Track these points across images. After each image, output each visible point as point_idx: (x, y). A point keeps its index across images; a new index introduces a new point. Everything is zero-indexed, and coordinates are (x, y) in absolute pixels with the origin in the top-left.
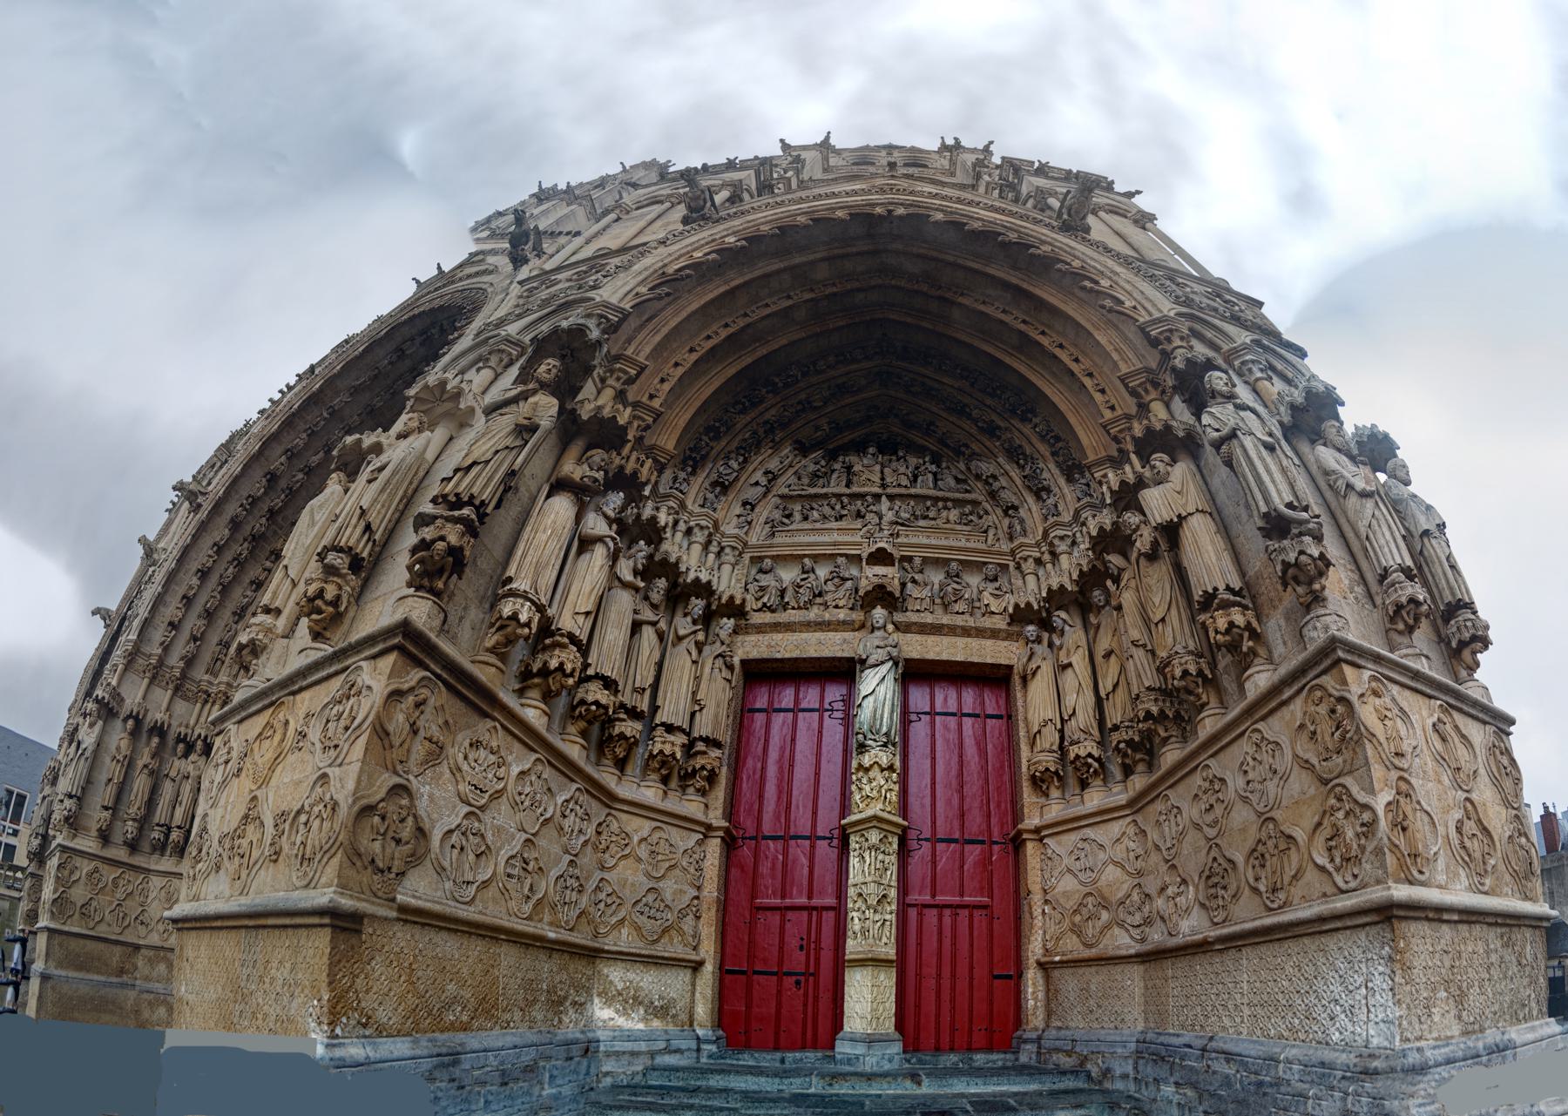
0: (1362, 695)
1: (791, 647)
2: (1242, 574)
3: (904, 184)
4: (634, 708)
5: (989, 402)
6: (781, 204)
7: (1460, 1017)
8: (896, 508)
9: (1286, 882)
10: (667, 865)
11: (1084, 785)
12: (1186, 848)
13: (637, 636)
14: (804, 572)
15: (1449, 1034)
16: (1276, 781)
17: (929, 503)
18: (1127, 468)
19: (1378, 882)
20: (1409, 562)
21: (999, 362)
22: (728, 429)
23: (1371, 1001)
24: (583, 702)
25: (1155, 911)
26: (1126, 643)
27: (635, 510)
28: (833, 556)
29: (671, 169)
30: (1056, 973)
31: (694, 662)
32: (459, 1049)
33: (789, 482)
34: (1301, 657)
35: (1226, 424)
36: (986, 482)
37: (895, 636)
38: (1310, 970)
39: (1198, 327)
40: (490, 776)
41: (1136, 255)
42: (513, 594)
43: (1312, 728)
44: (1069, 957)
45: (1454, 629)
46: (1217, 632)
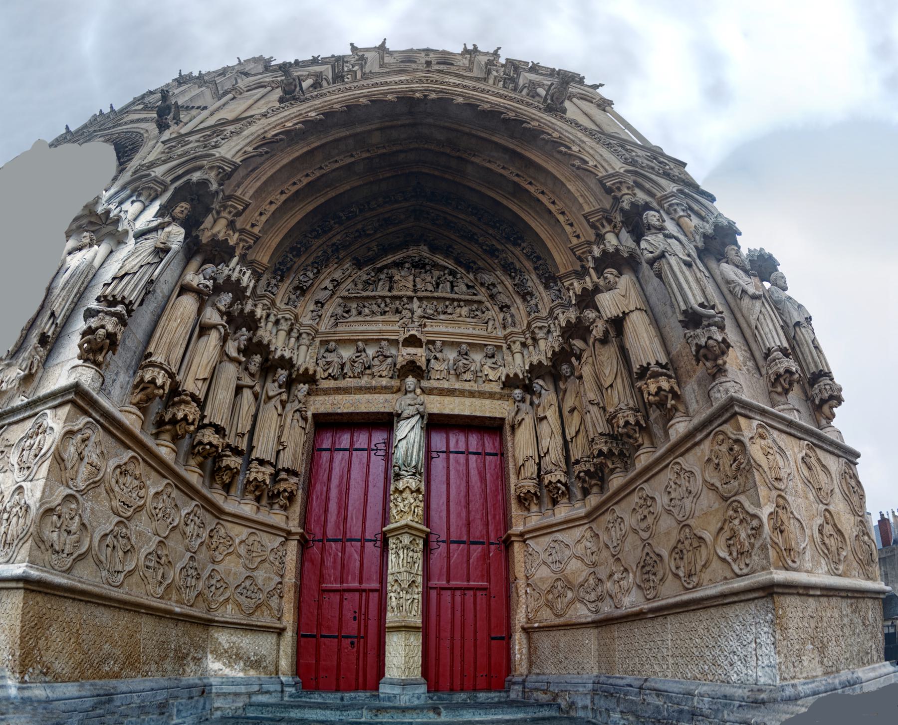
0: (752, 438)
2: (668, 353)
3: (436, 76)
4: (237, 447)
5: (491, 232)
6: (349, 89)
7: (822, 663)
8: (424, 306)
9: (698, 567)
10: (259, 559)
11: (555, 502)
12: (627, 546)
15: (814, 674)
16: (691, 498)
17: (447, 303)
18: (588, 279)
19: (764, 569)
20: (785, 344)
21: (499, 204)
22: (306, 249)
23: (759, 652)
24: (200, 443)
25: (605, 591)
26: (585, 402)
27: (240, 306)
29: (273, 63)
30: (535, 636)
31: (279, 415)
32: (112, 691)
34: (709, 411)
35: (657, 248)
36: (488, 288)
37: (422, 397)
38: (716, 631)
39: (640, 180)
40: (134, 495)
41: (597, 129)
42: (152, 365)
43: (716, 461)
44: (545, 624)
45: (817, 391)
46: (649, 394)
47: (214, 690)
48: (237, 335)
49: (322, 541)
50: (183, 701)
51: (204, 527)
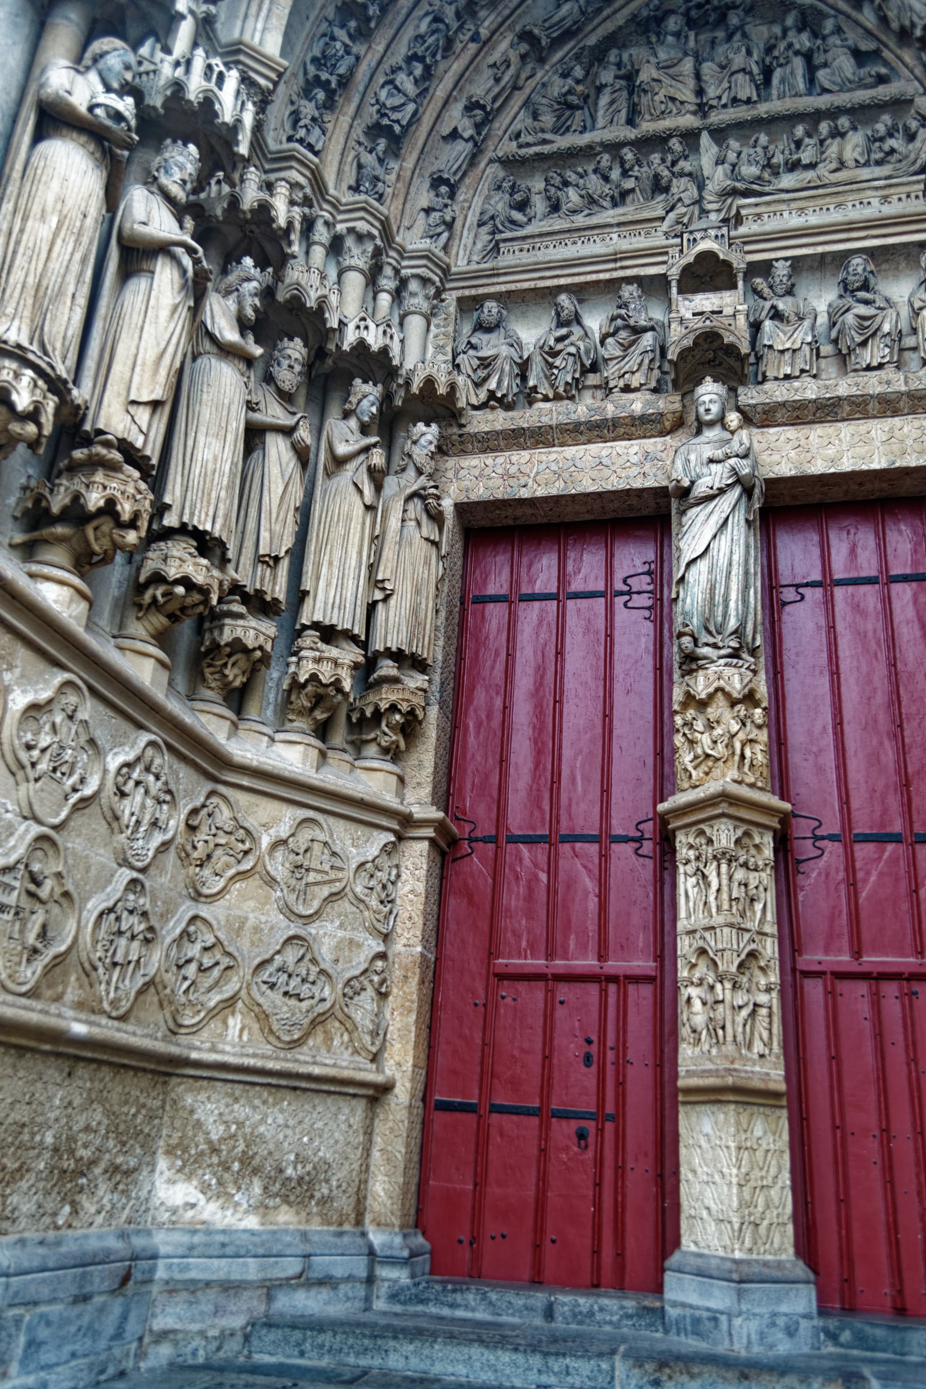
1: (548, 475)
4: (260, 593)
8: (732, 156)
13: (257, 454)
14: (560, 324)
24: (158, 578)
28: (613, 285)
31: (368, 508)
33: (517, 126)
37: (744, 434)
47: (161, 1273)
48: (232, 278)
49: (495, 840)
50: (55, 1310)
51: (173, 803)
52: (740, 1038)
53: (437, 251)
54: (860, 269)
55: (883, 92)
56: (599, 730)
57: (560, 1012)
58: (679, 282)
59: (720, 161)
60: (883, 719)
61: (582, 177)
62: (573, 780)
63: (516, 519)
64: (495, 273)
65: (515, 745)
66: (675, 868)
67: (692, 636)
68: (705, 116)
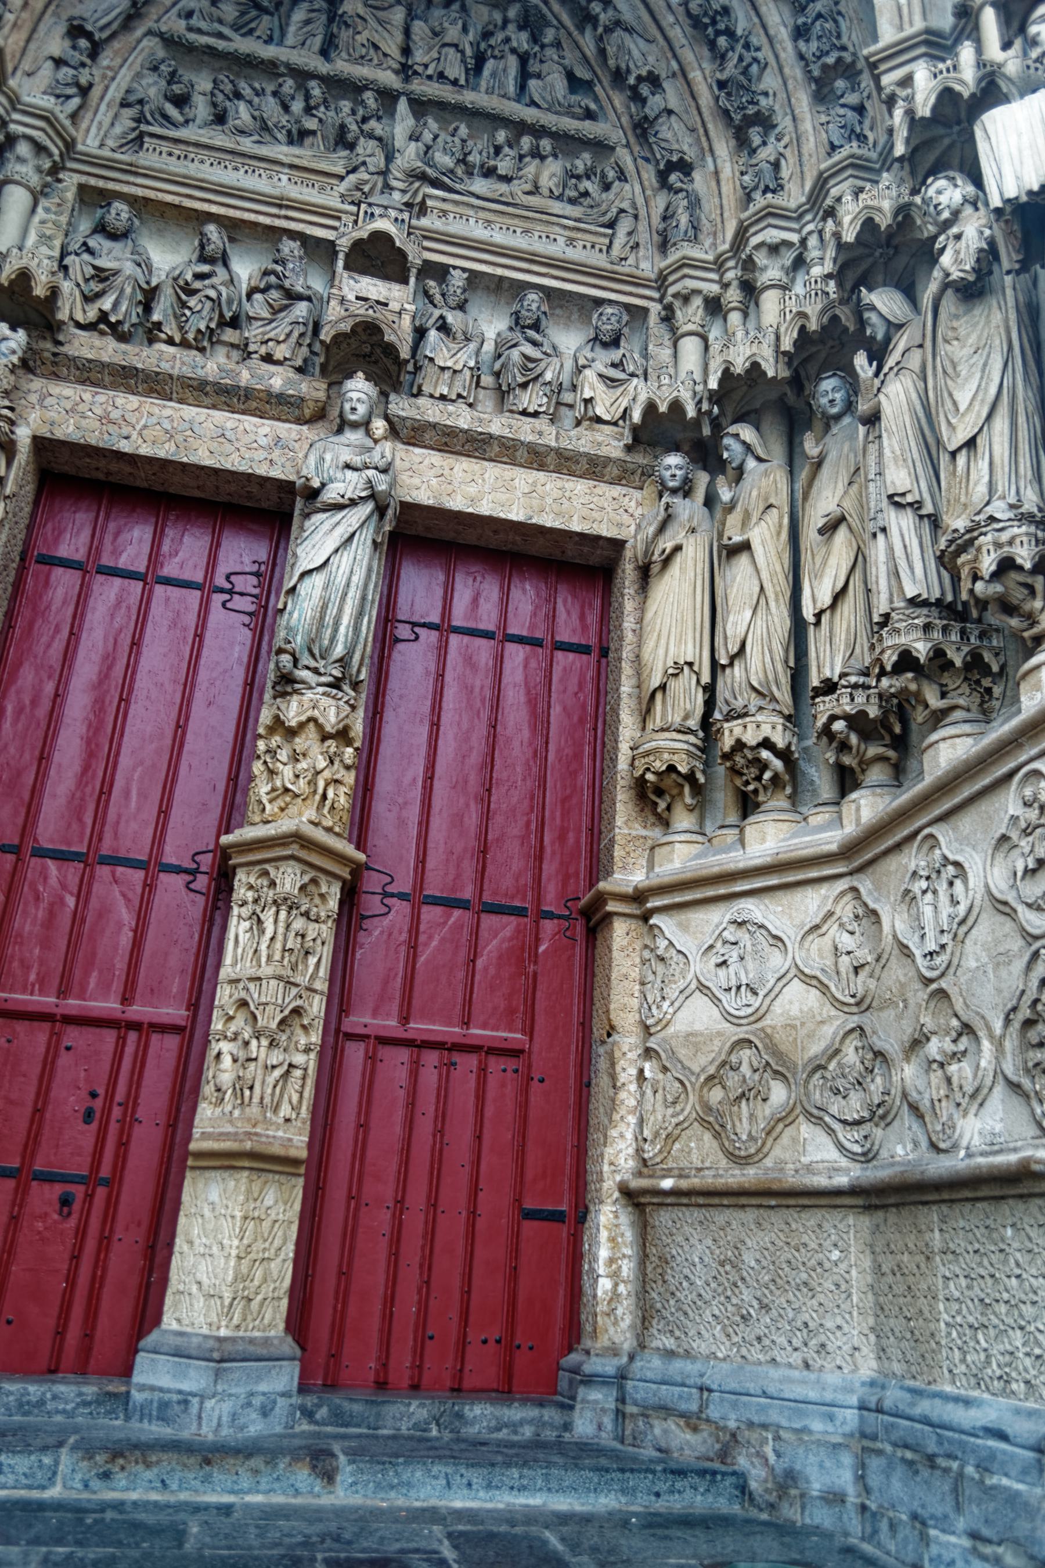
1: (157, 432)
8: (427, 137)
14: (203, 259)
17: (501, 136)
25: (896, 1091)
28: (273, 235)
30: (664, 1218)
37: (387, 446)
44: (695, 1182)
52: (267, 1100)
53: (62, 117)
54: (534, 306)
55: (589, 129)
56: (168, 741)
57: (64, 1060)
58: (347, 256)
59: (414, 137)
60: (473, 779)
61: (257, 95)
62: (127, 793)
63: (109, 474)
64: (132, 170)
65: (61, 741)
66: (229, 908)
67: (293, 655)
68: (407, 80)
